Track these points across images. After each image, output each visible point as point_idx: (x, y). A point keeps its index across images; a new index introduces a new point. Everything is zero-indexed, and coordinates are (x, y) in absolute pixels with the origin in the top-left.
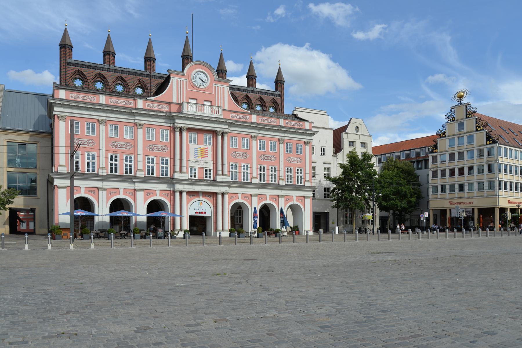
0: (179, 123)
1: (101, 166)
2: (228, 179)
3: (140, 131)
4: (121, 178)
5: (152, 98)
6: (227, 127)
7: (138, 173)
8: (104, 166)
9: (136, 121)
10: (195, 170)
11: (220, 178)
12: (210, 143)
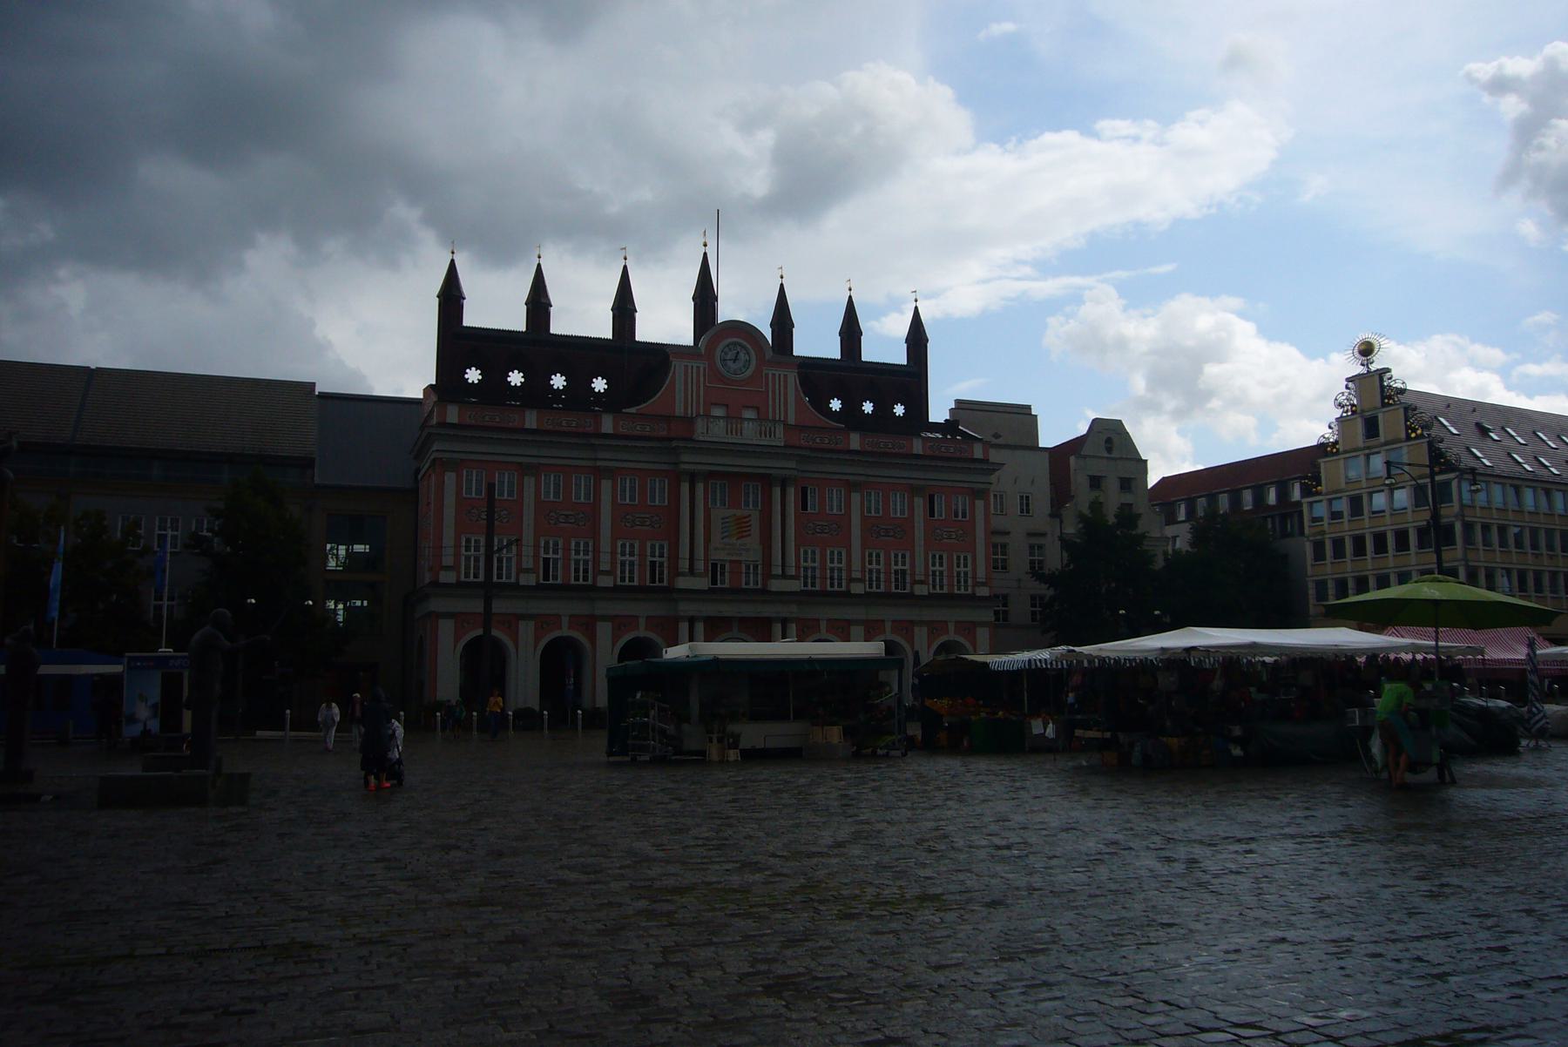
0: (689, 461)
1: (524, 566)
2: (796, 586)
3: (606, 485)
4: (566, 590)
5: (633, 410)
6: (792, 464)
7: (600, 578)
8: (531, 566)
9: (599, 463)
10: (723, 567)
11: (776, 585)
12: (755, 504)
